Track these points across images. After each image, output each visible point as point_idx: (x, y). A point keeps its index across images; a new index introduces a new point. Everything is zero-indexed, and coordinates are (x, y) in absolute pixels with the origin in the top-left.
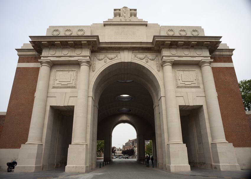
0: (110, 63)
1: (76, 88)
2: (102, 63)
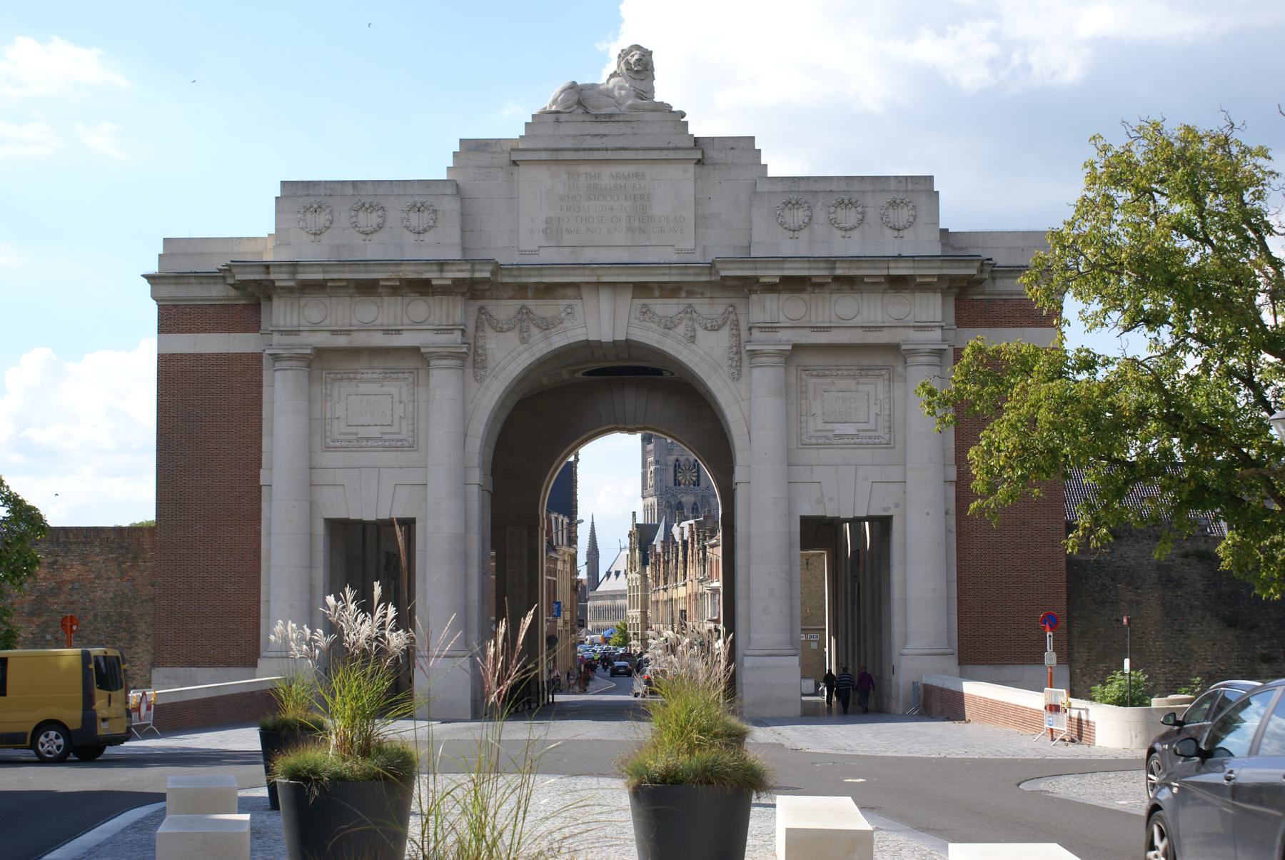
0: (542, 345)
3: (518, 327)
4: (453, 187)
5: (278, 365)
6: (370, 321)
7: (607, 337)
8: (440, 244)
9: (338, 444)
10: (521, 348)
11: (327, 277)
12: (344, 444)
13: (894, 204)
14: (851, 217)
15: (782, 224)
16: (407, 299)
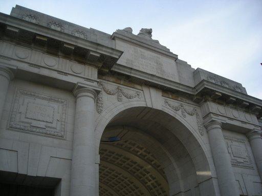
1: (64, 140)
2: (117, 102)
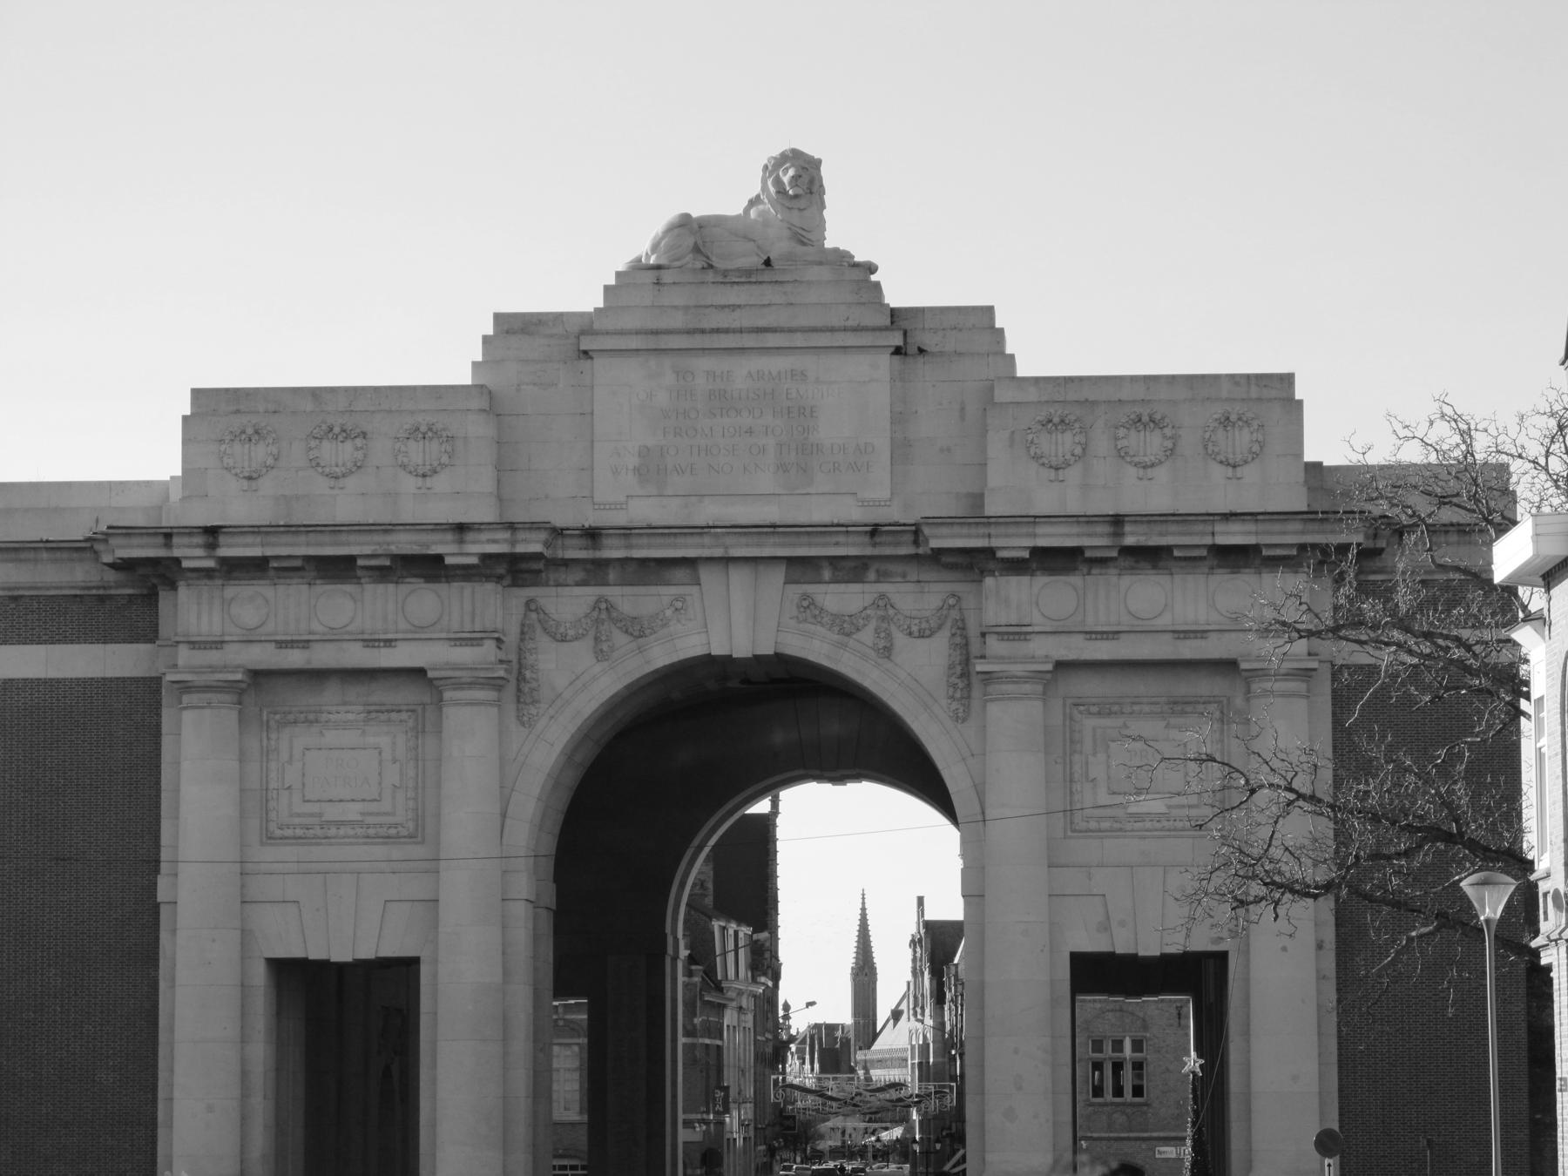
1: (423, 842)
3: (592, 633)
4: (484, 398)
5: (186, 699)
6: (340, 621)
7: (742, 648)
8: (458, 495)
9: (289, 832)
10: (598, 668)
11: (269, 552)
12: (299, 832)
13: (1226, 422)
14: (1153, 443)
15: (1036, 458)
16: (404, 588)
